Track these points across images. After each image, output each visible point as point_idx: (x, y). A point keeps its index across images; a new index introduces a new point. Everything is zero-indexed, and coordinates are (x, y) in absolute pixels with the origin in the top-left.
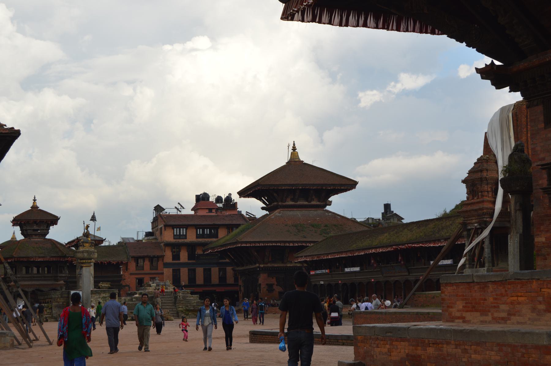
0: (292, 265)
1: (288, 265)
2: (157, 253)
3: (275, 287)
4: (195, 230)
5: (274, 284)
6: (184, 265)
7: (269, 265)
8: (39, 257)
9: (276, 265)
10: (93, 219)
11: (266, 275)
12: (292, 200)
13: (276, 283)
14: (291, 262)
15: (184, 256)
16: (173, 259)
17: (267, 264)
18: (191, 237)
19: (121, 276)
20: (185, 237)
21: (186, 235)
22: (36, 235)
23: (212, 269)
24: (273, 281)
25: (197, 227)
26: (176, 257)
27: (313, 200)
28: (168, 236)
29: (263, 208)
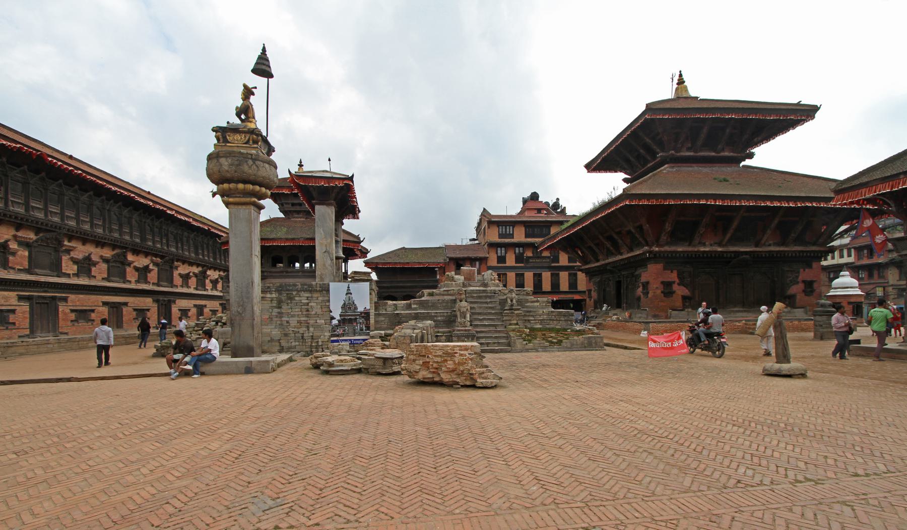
0: (707, 249)
1: (702, 249)
2: (481, 255)
3: (675, 287)
4: (523, 229)
5: (674, 282)
6: (511, 268)
7: (667, 248)
8: (287, 239)
9: (680, 249)
10: (262, 68)
11: (660, 266)
12: (689, 149)
13: (677, 281)
14: (704, 245)
15: (511, 260)
16: (498, 262)
17: (662, 246)
18: (519, 235)
19: (437, 281)
20: (512, 236)
21: (513, 234)
22: (298, 212)
23: (543, 274)
24: (673, 276)
25: (527, 225)
26: (502, 259)
27: (723, 150)
28: (493, 236)
29: (625, 180)
